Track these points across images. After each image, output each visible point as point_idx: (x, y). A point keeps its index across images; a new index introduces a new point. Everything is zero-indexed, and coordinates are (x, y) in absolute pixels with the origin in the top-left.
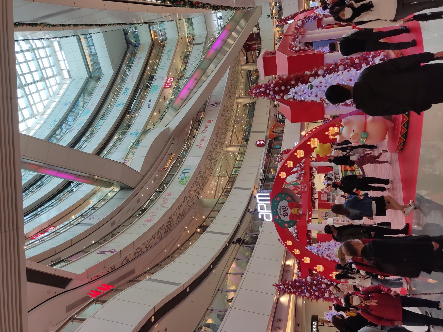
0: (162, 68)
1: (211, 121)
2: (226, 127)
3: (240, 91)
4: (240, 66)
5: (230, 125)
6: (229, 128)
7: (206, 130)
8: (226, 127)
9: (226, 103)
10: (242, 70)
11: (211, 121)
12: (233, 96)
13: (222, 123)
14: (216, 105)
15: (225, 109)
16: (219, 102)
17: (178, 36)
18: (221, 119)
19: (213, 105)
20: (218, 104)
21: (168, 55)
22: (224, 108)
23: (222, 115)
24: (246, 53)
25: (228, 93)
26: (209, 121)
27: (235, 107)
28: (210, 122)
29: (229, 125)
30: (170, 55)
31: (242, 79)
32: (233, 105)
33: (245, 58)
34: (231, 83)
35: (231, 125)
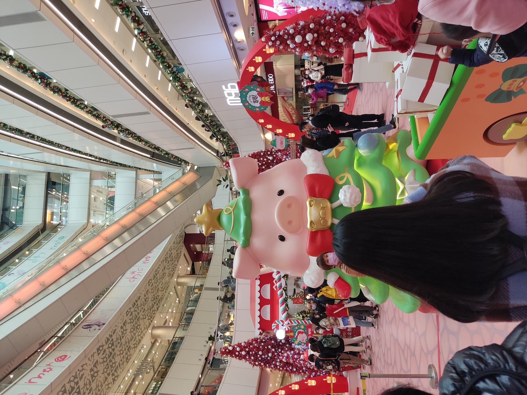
0: (34, 258)
1: (66, 356)
2: (106, 378)
3: (165, 317)
4: (175, 275)
5: (121, 378)
6: (117, 383)
7: (41, 378)
8: (106, 378)
9: (122, 328)
10: (179, 284)
11: (66, 356)
12: (146, 320)
13: (95, 366)
14: (93, 328)
15: (114, 337)
16: (104, 322)
17: (86, 221)
18: (93, 356)
19: (89, 326)
20: (99, 326)
21: (56, 243)
22: (111, 336)
23: (98, 349)
24: (193, 265)
25: (132, 310)
26: (61, 357)
27: (146, 342)
28: (63, 358)
29: (117, 376)
30: (59, 243)
31: (176, 300)
32: (142, 338)
33: (189, 269)
34: (145, 296)
35: (124, 378)
